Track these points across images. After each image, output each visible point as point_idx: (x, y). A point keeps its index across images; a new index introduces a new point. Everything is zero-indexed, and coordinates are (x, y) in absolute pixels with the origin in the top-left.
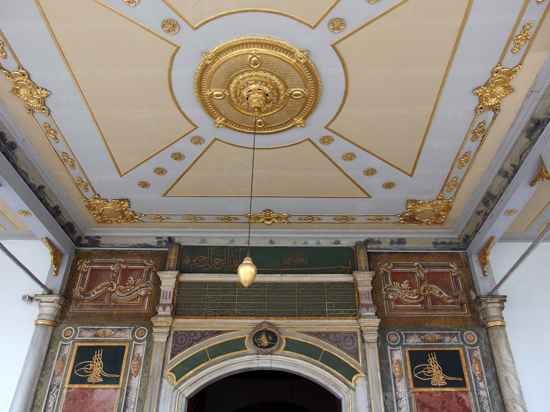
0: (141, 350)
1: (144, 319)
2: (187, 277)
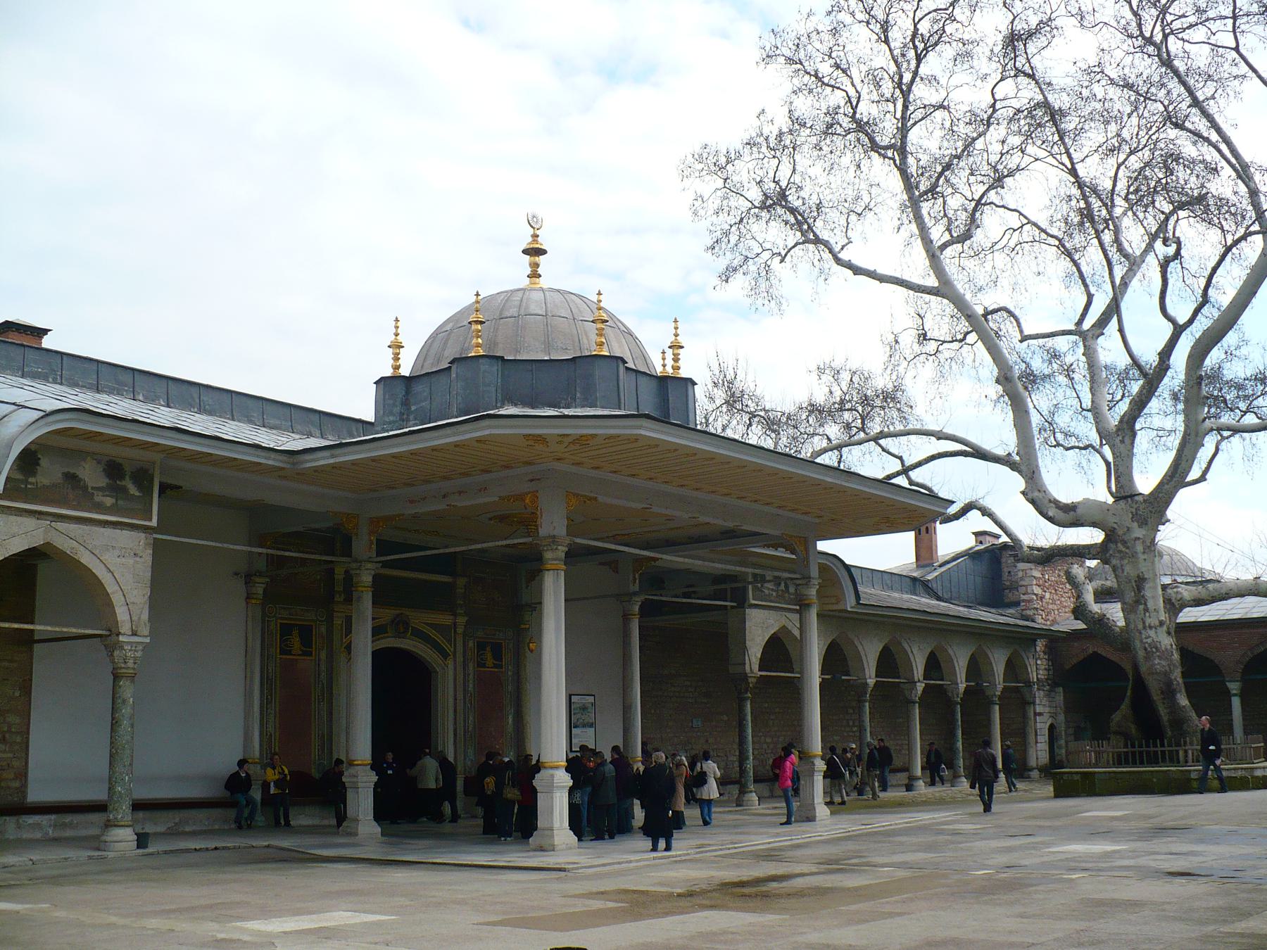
0: (323, 629)
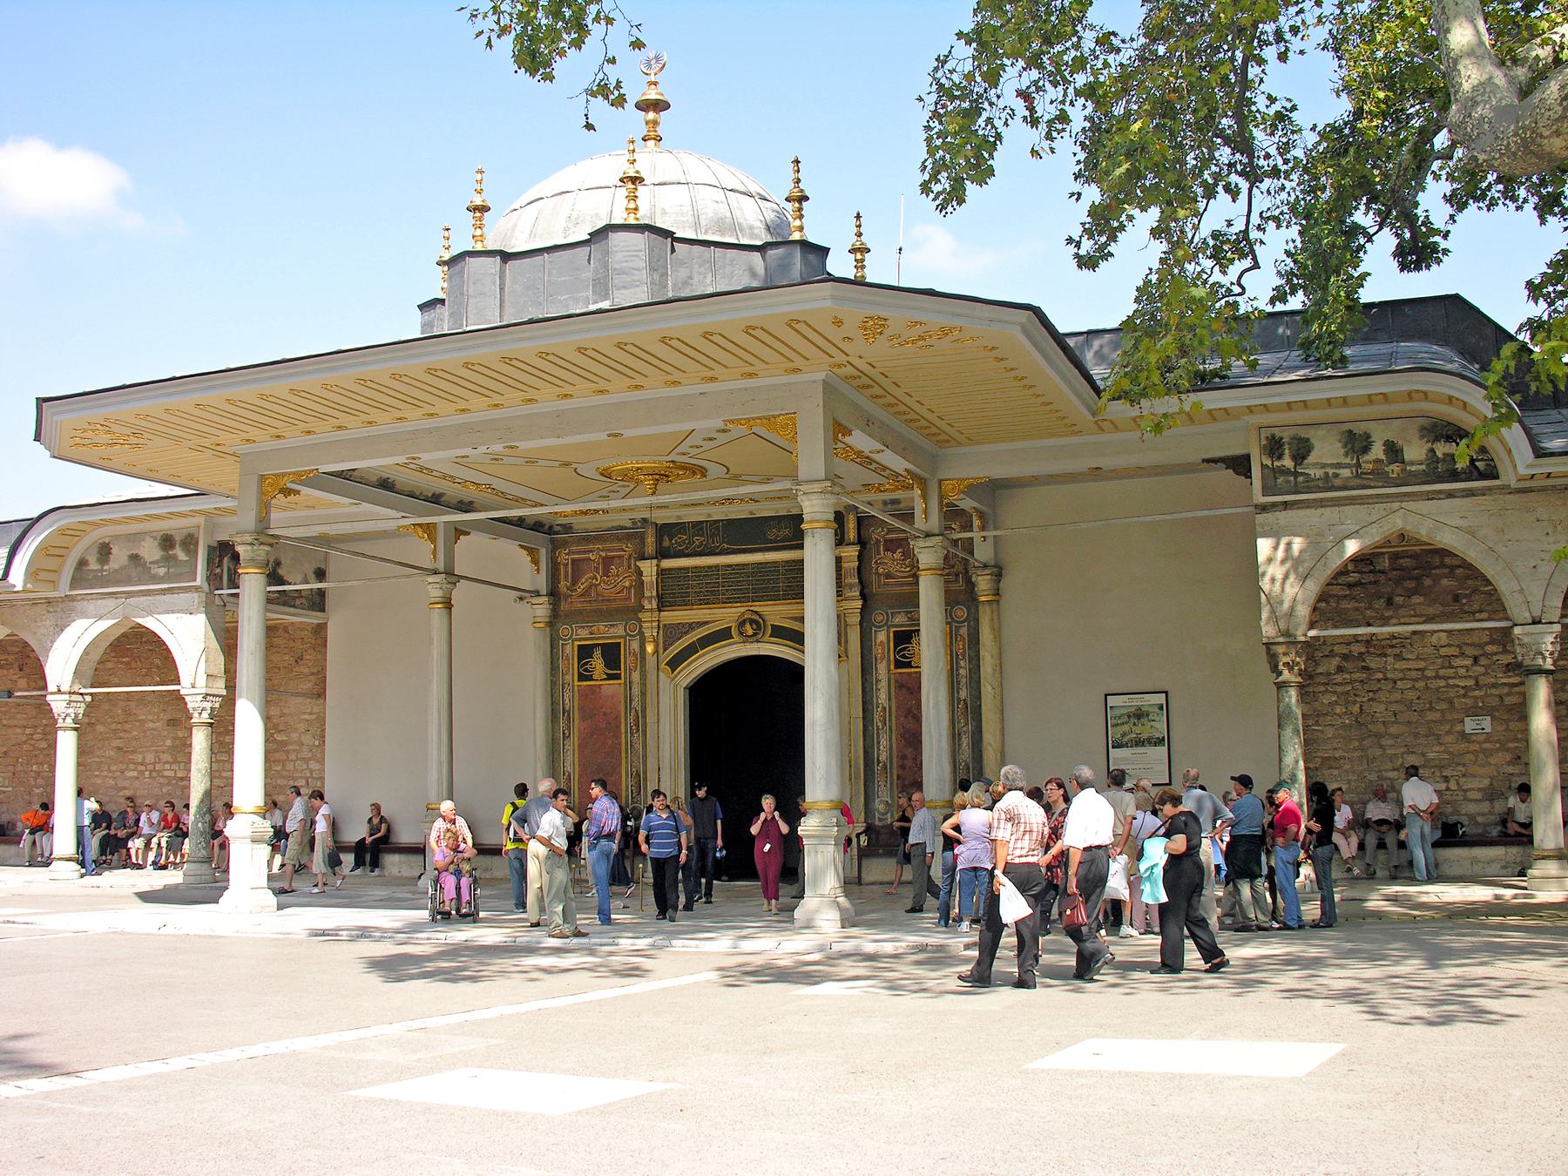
0: (635, 645)
1: (631, 613)
2: (668, 563)
